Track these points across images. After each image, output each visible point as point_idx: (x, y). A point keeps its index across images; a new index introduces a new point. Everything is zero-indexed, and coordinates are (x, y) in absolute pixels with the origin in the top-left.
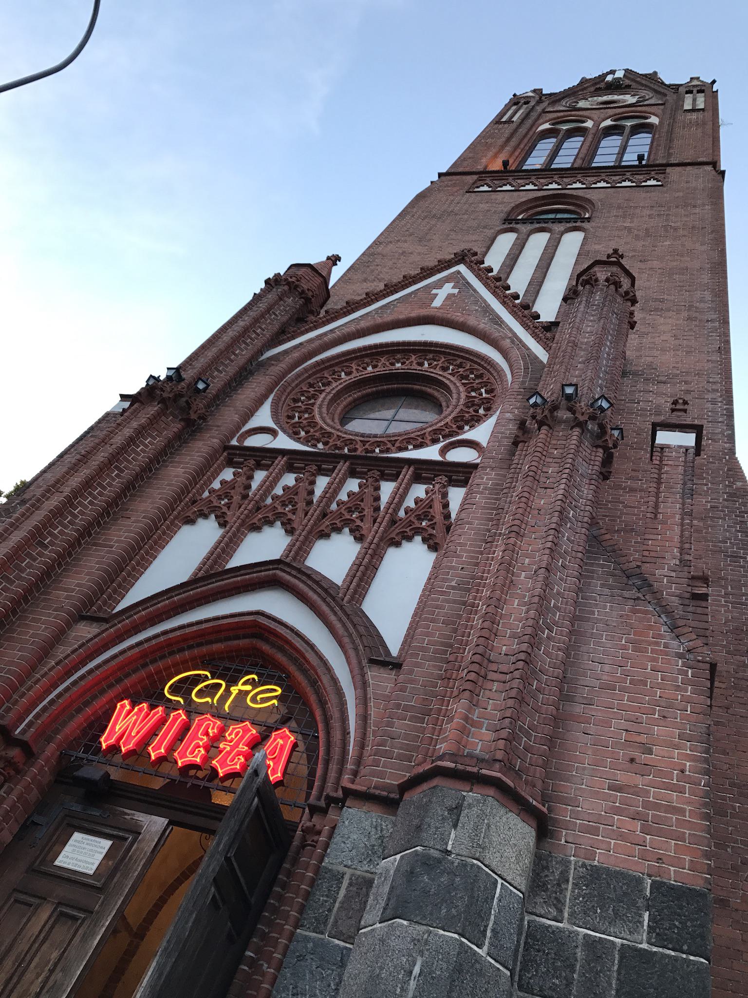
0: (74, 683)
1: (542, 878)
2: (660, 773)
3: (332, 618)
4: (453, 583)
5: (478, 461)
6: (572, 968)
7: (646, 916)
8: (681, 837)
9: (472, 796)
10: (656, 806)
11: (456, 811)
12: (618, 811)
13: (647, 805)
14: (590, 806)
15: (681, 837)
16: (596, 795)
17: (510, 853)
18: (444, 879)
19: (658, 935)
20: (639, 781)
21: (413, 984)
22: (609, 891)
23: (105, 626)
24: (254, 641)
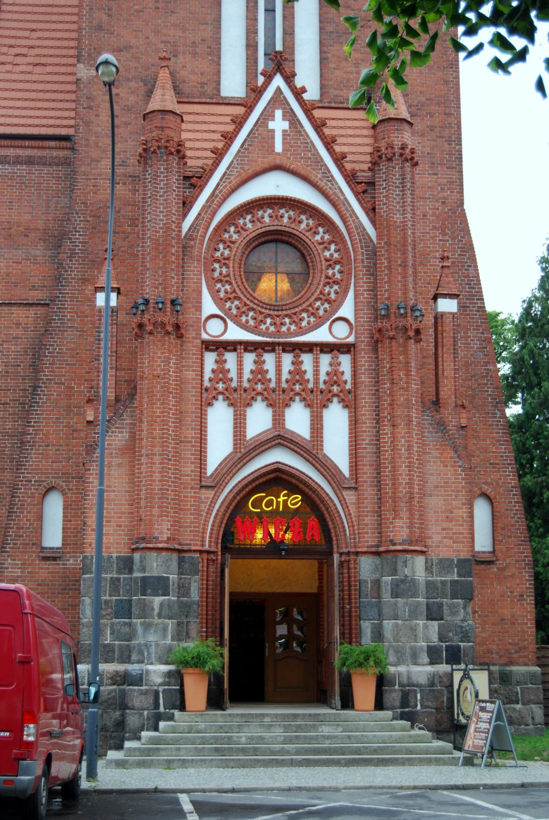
0: (215, 518)
1: (428, 569)
2: (457, 521)
3: (317, 465)
4: (367, 442)
5: (351, 339)
6: (438, 590)
7: (456, 569)
8: (463, 542)
9: (409, 556)
10: (456, 533)
11: (405, 563)
12: (445, 538)
13: (454, 533)
14: (436, 538)
15: (463, 542)
16: (438, 533)
17: (421, 568)
18: (408, 585)
19: (459, 575)
20: (450, 525)
21: (407, 614)
22: (445, 565)
23: (216, 489)
24: (278, 473)
